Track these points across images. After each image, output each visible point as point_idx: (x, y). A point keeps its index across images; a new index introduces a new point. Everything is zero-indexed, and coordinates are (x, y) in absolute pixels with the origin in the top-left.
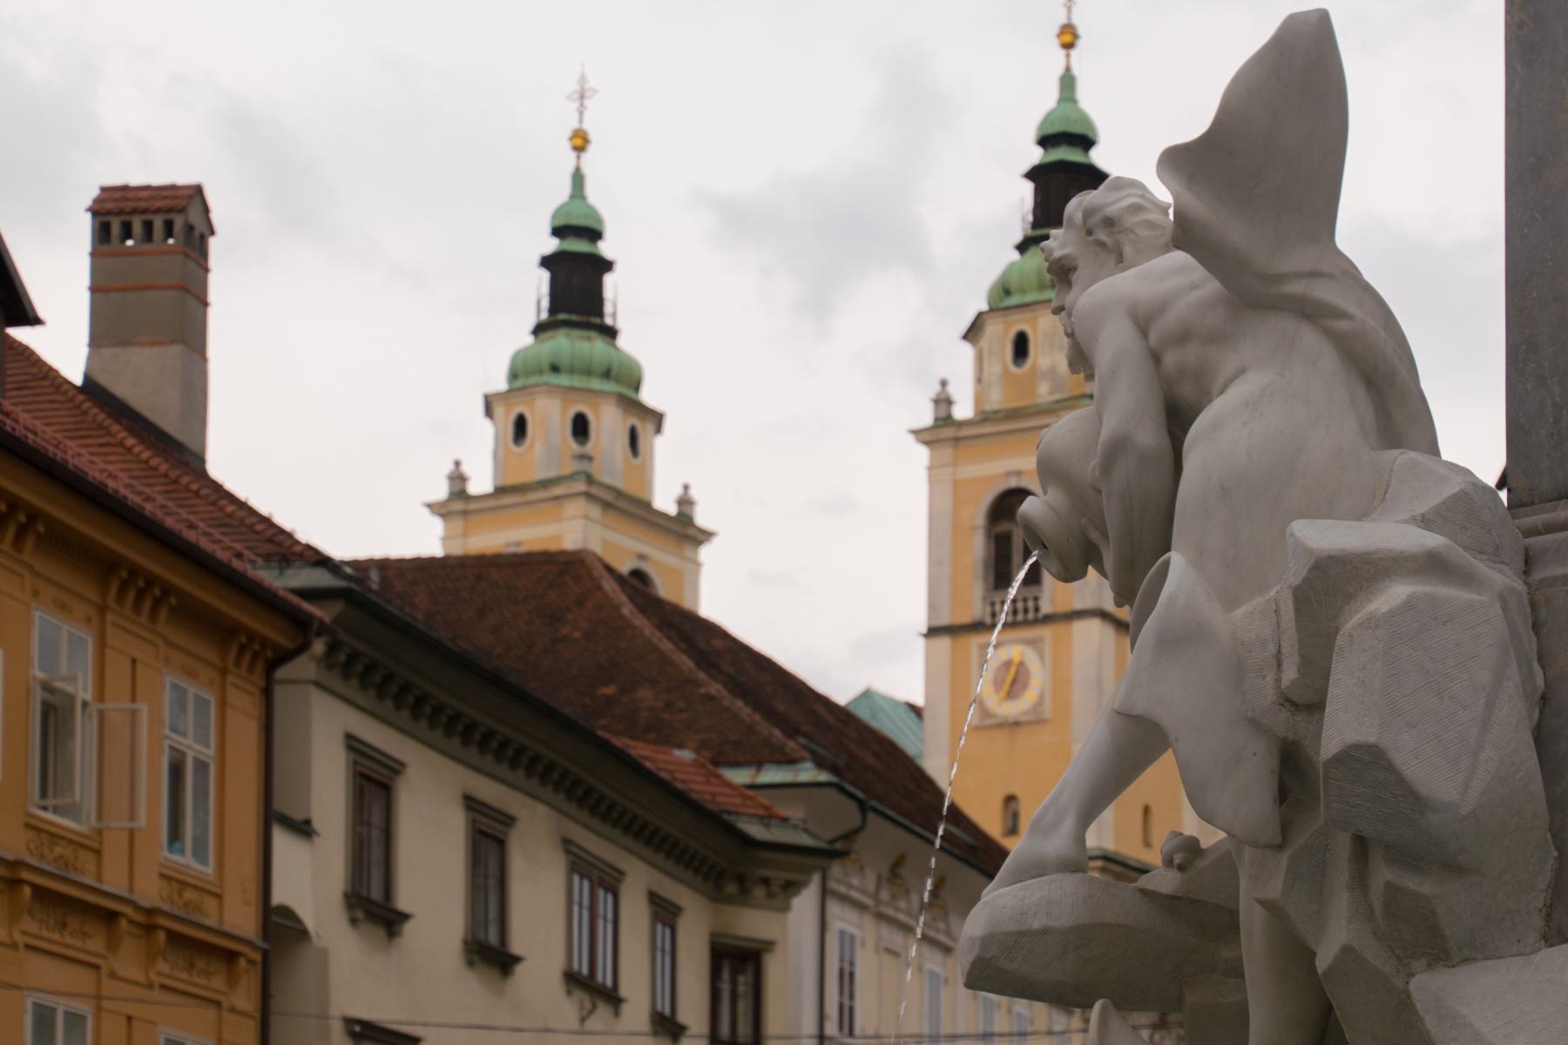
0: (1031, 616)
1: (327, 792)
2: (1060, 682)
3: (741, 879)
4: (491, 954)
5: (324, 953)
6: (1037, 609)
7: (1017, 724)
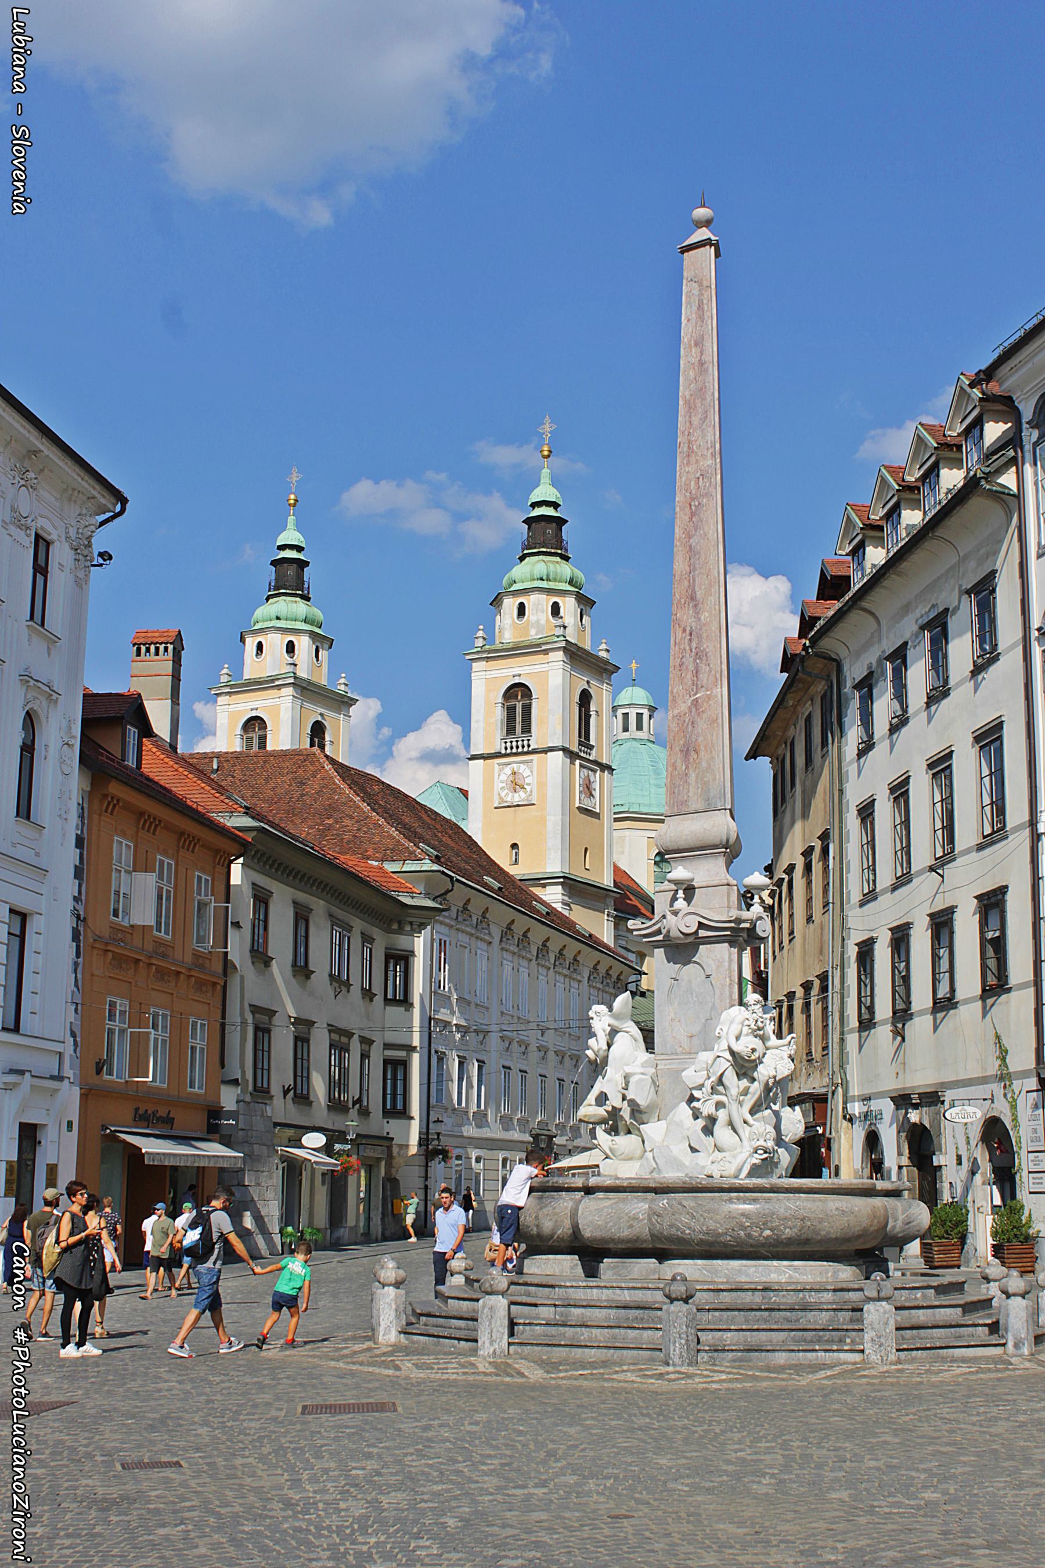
0: (526, 749)
1: (245, 909)
2: (542, 785)
3: (399, 923)
4: (302, 970)
5: (242, 977)
6: (529, 746)
7: (518, 806)
